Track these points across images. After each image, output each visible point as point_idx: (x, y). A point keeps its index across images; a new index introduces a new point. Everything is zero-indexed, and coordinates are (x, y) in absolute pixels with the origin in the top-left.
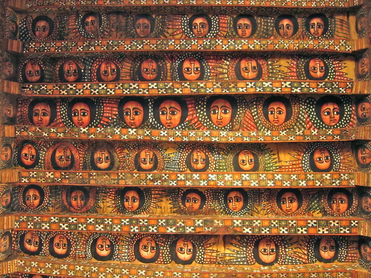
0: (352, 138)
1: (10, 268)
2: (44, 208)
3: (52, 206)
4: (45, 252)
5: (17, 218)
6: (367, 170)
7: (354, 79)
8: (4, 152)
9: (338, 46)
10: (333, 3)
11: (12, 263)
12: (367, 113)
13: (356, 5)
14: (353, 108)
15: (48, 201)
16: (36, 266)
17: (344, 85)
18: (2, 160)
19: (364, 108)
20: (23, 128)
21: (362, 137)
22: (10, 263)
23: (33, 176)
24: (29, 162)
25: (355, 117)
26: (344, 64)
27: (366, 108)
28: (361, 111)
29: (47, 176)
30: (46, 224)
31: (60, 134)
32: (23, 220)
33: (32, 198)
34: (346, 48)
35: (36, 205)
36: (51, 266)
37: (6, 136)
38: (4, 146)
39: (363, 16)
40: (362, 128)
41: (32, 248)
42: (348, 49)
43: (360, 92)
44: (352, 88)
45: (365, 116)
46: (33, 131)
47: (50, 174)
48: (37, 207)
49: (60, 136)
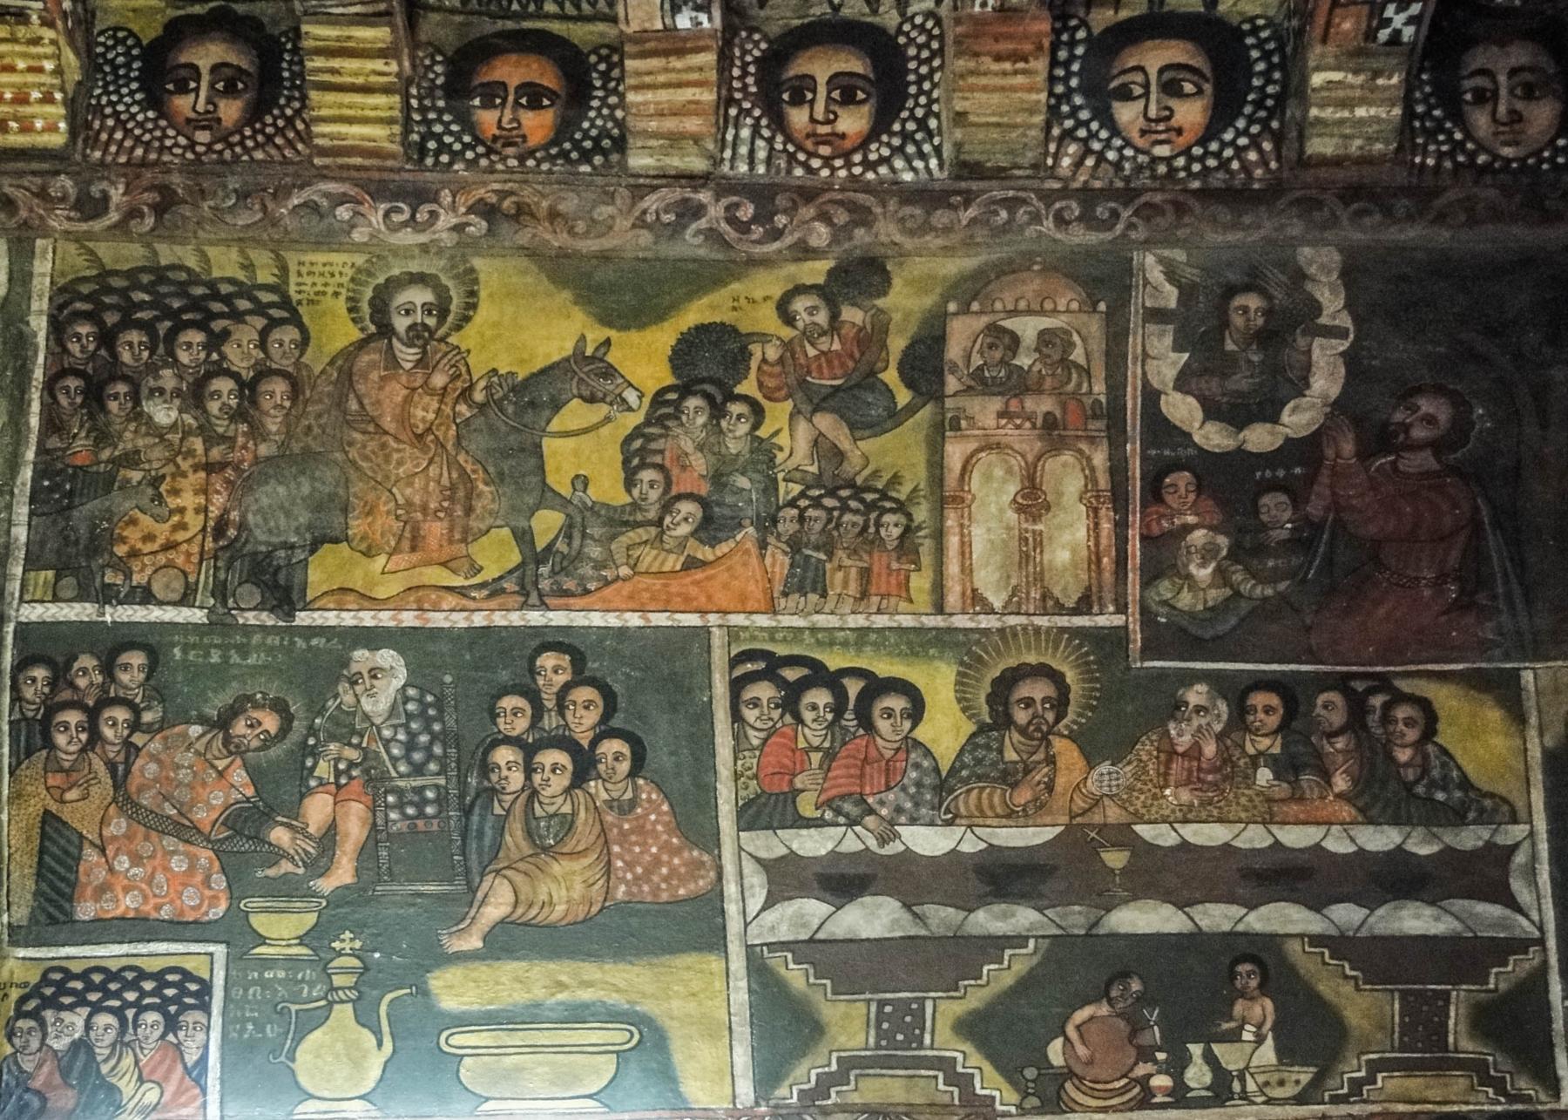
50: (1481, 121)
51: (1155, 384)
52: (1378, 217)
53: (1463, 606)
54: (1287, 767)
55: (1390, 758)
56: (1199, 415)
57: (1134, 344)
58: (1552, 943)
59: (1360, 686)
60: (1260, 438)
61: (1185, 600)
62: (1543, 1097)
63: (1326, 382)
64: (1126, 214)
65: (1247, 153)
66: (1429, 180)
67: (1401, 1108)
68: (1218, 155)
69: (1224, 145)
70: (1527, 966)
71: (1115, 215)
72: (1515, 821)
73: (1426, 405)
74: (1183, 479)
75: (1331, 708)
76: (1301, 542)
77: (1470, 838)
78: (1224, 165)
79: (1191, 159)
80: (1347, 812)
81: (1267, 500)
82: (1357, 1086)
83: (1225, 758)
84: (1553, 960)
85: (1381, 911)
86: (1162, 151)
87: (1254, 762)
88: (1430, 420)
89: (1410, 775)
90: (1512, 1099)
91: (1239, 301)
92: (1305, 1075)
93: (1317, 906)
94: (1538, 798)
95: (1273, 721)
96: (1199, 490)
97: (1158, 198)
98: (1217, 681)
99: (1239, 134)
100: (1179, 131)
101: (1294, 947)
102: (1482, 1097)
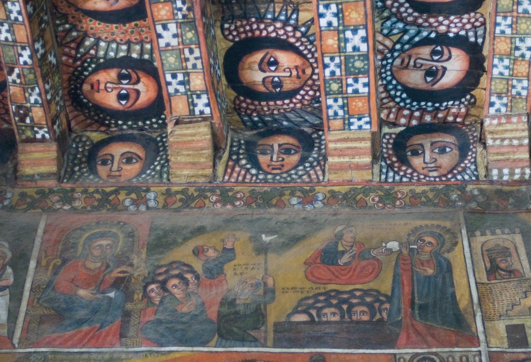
1: (511, 139)
2: (304, 35)
3: (296, 10)
4: (468, 26)
5: (337, 123)
8: (115, 167)
11: (496, 132)
15: (278, 25)
16: (506, 62)
18: (139, 175)
20: (23, 120)
22: (495, 139)
23: (181, 83)
24: (145, 85)
29: (174, 42)
30: (346, 40)
31: (11, 12)
32: (342, 107)
33: (273, 73)
35: (298, 61)
36: (505, 18)
37: (54, 169)
38: (93, 171)
41: (455, 66)
46: (24, 90)
47: (165, 33)
48: (304, 56)
49: (19, 13)
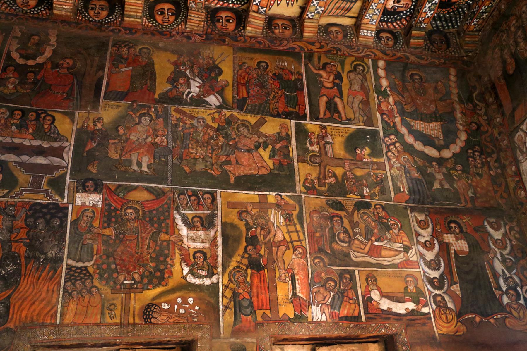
0: (191, 3)
6: (146, 15)
7: (270, 12)
9: (316, 5)
10: (375, 8)
12: (222, 25)
13: (360, 32)
14: (231, 5)
17: (264, 5)
19: (228, 21)
21: (191, 16)
25: (219, 5)
26: (292, 5)
27: (228, 24)
28: (226, 17)
34: (311, 13)
39: (345, 36)
40: (202, 15)
42: (309, 15)
43: (250, 22)
44: (257, 12)
45: (218, 21)
50: (92, 13)
51: (11, 49)
52: (68, 26)
53: (67, 98)
54: (19, 127)
55: (43, 127)
56: (19, 56)
57: (9, 42)
58: (69, 167)
59: (40, 112)
60: (31, 62)
61: (6, 91)
62: (60, 200)
63: (48, 54)
64: (15, 19)
65: (42, 10)
66: (79, 21)
67: (27, 200)
68: (37, 11)
69: (39, 9)
70: (63, 172)
71: (12, 19)
72: (67, 141)
73: (67, 61)
74: (12, 68)
75: (32, 116)
76: (35, 83)
77: (56, 144)
78: (38, 13)
79: (31, 11)
80: (30, 137)
81: (29, 74)
82: (17, 195)
83: (6, 123)
84: (69, 171)
85: (32, 158)
86: (25, 9)
87: (12, 125)
88: (68, 63)
89: (47, 130)
90: (53, 200)
91: (33, 37)
92: (5, 191)
93: (18, 155)
94: (73, 137)
95: (19, 117)
96: (15, 71)
97: (23, 17)
98: (8, 108)
99: (42, 8)
100: (29, 6)
101: (10, 164)
102: (46, 199)
